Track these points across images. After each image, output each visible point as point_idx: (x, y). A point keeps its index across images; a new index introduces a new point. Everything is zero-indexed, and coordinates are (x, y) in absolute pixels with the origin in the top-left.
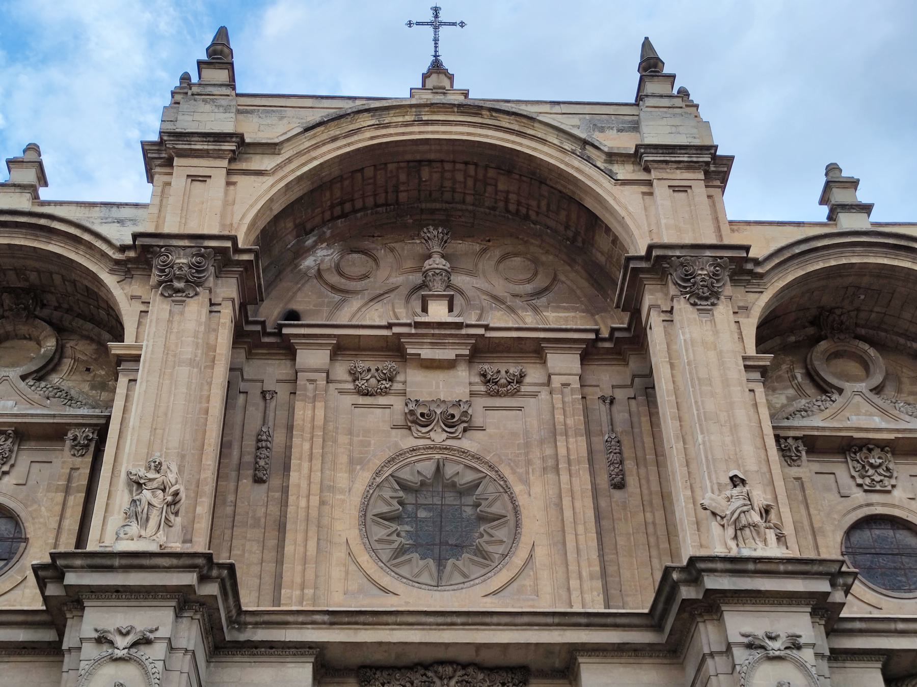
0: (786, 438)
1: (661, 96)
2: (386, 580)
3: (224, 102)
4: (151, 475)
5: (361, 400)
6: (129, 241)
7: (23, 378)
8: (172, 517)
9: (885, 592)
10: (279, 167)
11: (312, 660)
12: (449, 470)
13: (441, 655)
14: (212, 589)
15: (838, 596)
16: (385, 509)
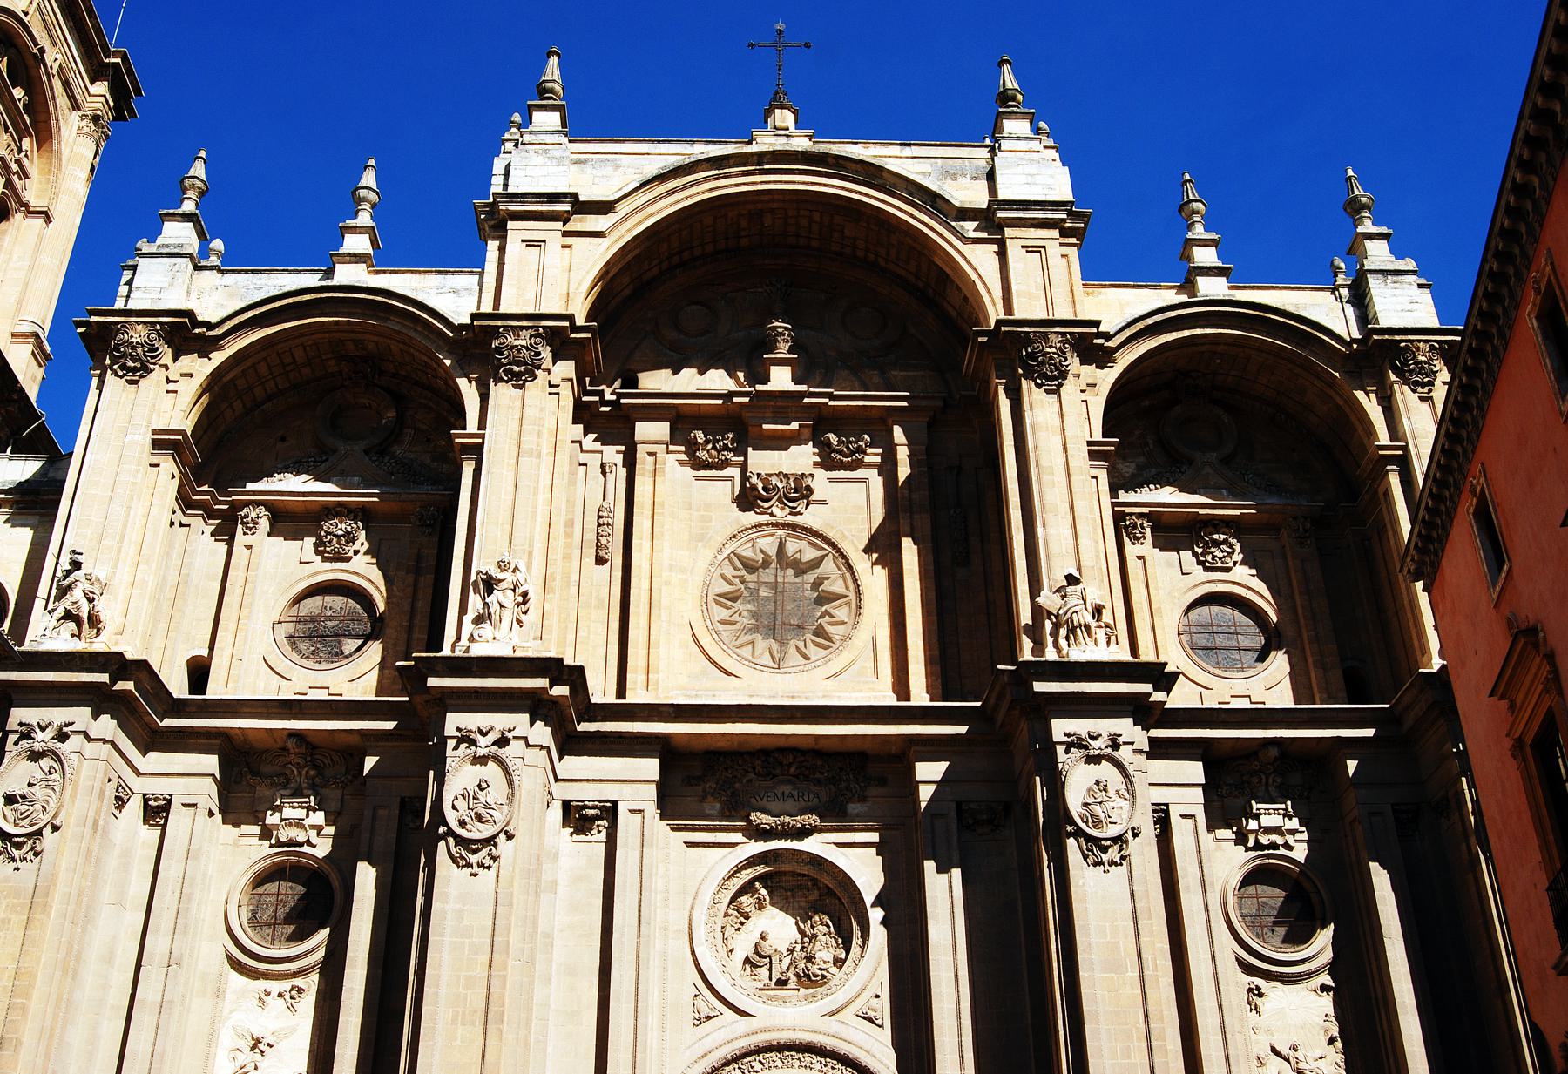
0: (1131, 514)
1: (1018, 138)
2: (727, 664)
3: (555, 152)
4: (500, 576)
5: (702, 473)
6: (468, 321)
7: (367, 452)
8: (523, 617)
9: (1217, 671)
10: (615, 226)
11: (659, 747)
12: (792, 546)
13: (782, 743)
14: (561, 691)
15: (1158, 696)
16: (727, 588)
